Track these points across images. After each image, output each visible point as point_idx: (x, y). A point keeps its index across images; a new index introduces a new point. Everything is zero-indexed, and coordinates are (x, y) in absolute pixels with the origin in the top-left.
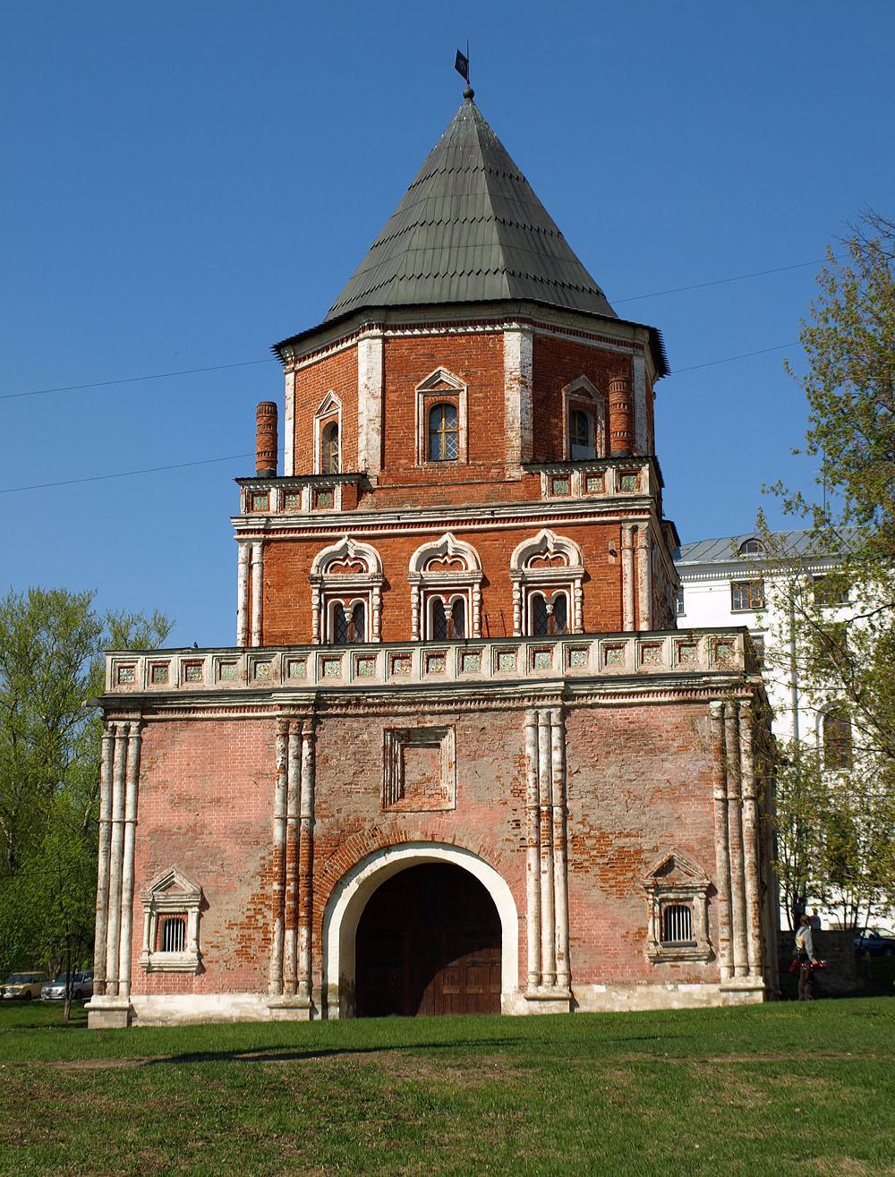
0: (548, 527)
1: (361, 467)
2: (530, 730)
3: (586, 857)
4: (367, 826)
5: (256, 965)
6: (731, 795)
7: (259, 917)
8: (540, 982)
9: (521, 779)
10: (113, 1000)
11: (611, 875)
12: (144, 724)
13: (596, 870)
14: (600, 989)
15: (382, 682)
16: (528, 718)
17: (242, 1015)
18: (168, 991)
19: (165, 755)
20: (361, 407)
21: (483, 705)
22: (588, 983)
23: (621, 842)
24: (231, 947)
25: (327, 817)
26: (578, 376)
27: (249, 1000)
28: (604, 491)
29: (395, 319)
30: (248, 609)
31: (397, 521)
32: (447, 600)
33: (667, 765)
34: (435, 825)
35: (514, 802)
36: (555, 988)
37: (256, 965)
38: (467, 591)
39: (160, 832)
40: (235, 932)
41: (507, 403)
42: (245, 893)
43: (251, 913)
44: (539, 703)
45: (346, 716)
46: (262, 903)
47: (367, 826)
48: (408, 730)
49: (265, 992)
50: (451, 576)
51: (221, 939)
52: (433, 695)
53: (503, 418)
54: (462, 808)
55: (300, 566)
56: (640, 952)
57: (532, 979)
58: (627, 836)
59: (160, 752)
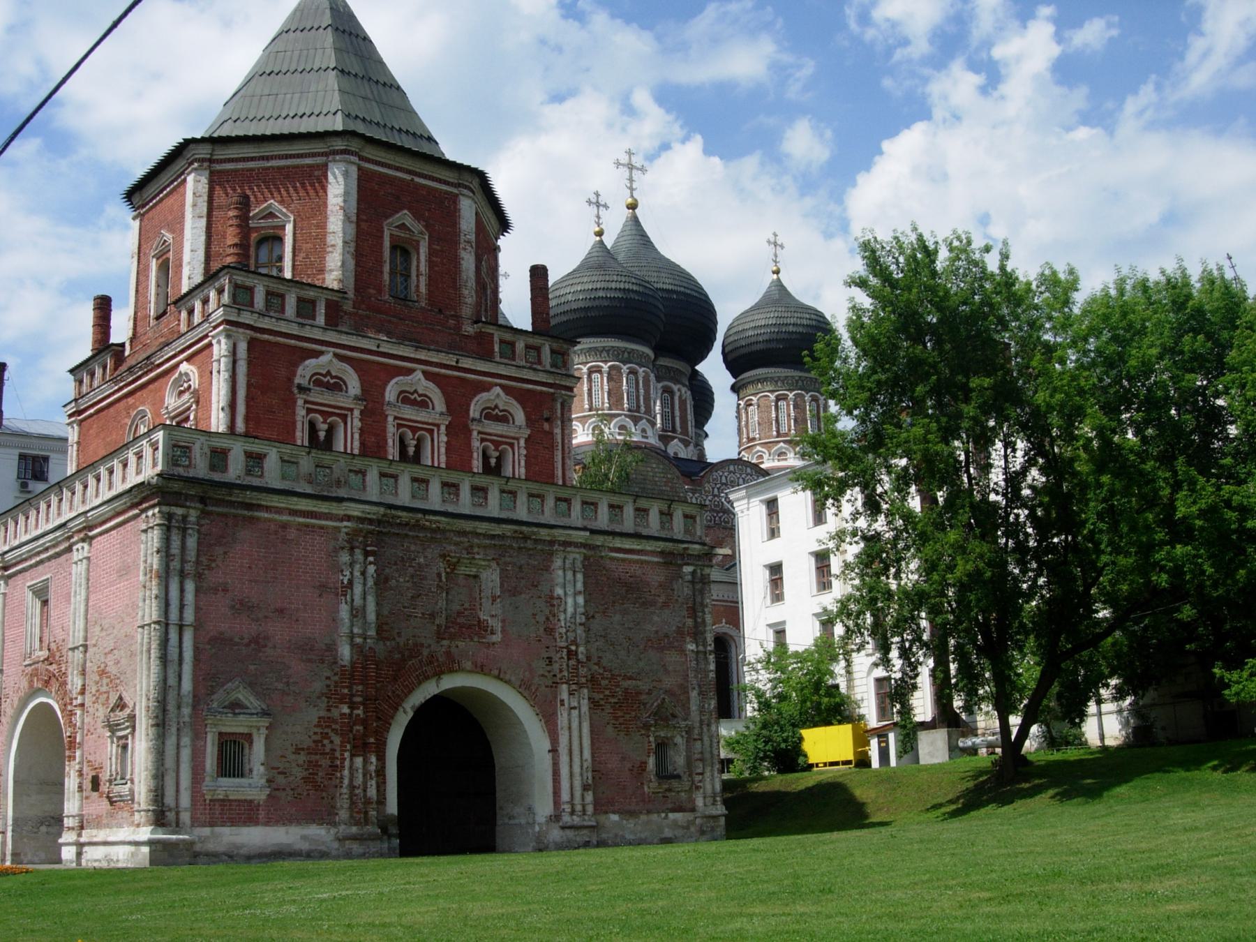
0: (496, 385)
2: (560, 572)
3: (602, 696)
4: (425, 652)
5: (324, 794)
6: (701, 648)
7: (326, 742)
8: (573, 813)
9: (551, 618)
11: (620, 714)
12: (204, 514)
13: (608, 709)
14: (615, 817)
16: (558, 562)
17: (313, 847)
18: (233, 822)
19: (225, 553)
22: (606, 813)
24: (298, 773)
25: (388, 639)
27: (318, 832)
28: (540, 362)
29: (370, 152)
30: (232, 405)
31: (375, 348)
32: (414, 436)
36: (586, 818)
37: (324, 794)
38: (431, 432)
39: (220, 640)
40: (302, 758)
41: (462, 262)
42: (314, 714)
43: (318, 737)
44: (569, 549)
46: (327, 727)
47: (425, 652)
49: (334, 824)
50: (421, 416)
51: (287, 765)
52: (483, 527)
57: (567, 808)
58: (631, 678)
59: (219, 550)
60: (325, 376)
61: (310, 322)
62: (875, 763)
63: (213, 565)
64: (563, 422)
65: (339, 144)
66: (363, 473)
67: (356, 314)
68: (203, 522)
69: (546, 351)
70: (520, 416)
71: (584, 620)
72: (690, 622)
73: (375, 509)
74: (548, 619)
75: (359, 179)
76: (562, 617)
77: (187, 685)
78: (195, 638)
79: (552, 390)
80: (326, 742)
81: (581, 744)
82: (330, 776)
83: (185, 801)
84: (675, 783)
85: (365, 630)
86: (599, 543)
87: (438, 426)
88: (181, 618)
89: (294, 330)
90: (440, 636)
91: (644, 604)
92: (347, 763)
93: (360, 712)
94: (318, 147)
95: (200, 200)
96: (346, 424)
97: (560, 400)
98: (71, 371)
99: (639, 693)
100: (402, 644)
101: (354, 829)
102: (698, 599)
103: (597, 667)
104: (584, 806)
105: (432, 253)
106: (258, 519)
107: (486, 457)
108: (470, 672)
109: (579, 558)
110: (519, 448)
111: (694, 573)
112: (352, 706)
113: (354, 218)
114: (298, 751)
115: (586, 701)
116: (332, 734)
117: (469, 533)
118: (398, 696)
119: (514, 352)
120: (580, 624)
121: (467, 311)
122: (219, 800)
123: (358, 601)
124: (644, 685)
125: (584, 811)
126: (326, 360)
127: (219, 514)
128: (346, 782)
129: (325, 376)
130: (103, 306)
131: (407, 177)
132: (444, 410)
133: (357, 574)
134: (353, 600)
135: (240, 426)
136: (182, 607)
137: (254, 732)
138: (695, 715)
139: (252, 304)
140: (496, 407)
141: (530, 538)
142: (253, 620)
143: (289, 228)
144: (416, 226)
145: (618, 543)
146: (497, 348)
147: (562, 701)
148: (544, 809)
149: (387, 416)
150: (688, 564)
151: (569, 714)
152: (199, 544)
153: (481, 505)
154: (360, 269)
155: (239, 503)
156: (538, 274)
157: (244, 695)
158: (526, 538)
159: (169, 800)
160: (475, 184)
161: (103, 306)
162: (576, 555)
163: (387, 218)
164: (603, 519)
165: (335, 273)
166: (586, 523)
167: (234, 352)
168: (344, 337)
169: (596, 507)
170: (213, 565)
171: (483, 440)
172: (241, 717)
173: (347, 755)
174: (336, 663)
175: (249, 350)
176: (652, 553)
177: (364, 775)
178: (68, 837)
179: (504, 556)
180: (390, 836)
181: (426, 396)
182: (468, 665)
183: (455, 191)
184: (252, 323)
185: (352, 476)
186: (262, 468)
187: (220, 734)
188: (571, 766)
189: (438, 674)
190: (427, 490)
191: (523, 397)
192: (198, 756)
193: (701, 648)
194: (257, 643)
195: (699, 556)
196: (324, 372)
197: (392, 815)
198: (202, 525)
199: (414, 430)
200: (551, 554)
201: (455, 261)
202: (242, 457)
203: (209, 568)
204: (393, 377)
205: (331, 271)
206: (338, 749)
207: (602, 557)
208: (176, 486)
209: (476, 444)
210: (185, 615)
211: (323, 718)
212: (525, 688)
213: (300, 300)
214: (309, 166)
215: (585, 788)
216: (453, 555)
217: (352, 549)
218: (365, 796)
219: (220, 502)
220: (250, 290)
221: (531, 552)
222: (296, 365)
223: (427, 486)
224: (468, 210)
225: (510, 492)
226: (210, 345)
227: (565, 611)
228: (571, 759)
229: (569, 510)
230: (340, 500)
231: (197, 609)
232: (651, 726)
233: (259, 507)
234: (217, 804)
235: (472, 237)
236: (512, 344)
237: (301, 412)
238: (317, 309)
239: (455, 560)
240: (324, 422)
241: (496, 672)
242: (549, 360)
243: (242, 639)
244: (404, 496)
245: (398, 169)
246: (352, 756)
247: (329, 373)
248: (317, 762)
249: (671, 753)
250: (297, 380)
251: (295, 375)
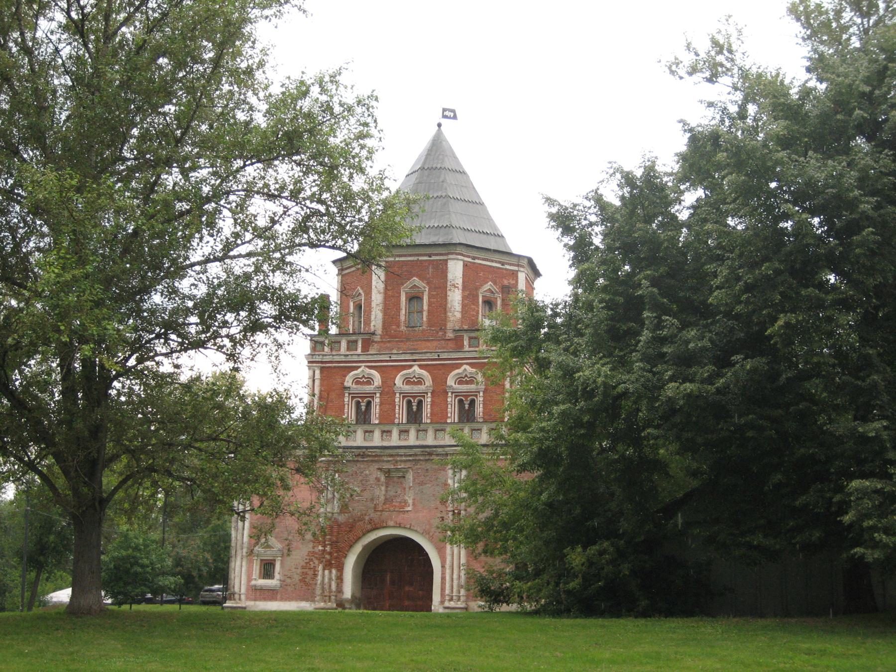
1: (372, 329)
4: (367, 518)
7: (311, 563)
10: (237, 603)
18: (265, 599)
20: (373, 298)
21: (427, 458)
24: (297, 578)
26: (487, 282)
34: (400, 518)
35: (442, 508)
36: (459, 603)
40: (299, 571)
43: (307, 561)
47: (367, 518)
48: (389, 469)
49: (313, 601)
53: (446, 305)
55: (339, 381)
57: (447, 598)
67: (382, 342)
80: (311, 563)
83: (243, 590)
87: (427, 393)
89: (343, 358)
90: (376, 511)
92: (320, 573)
93: (328, 549)
112: (325, 546)
113: (382, 291)
116: (314, 559)
117: (396, 455)
121: (450, 325)
126: (362, 370)
128: (319, 582)
131: (415, 258)
140: (466, 376)
146: (466, 343)
153: (406, 439)
158: (430, 454)
175: (321, 372)
182: (391, 523)
183: (445, 258)
187: (262, 560)
213: (349, 342)
222: (345, 376)
235: (459, 281)
241: (408, 526)
245: (410, 255)
246: (324, 569)
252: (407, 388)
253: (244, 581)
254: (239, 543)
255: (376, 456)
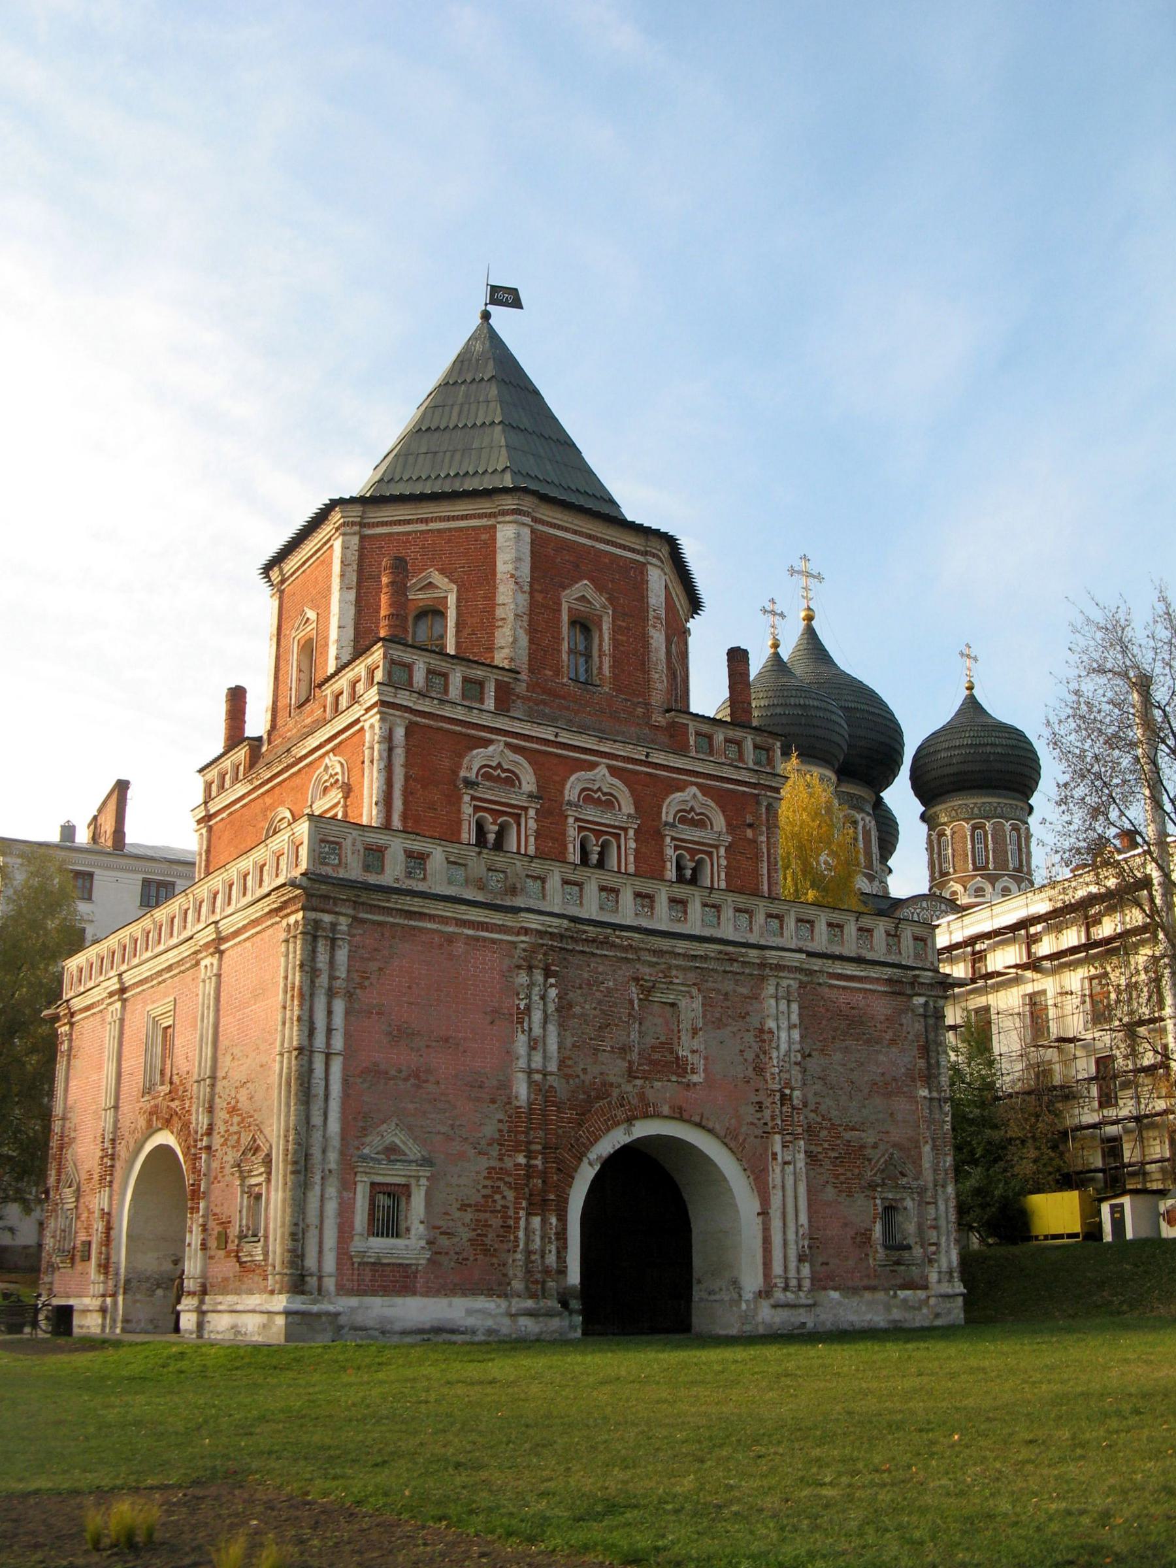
0: (696, 784)
2: (773, 1002)
4: (615, 1093)
5: (495, 1260)
7: (497, 1197)
8: (786, 1288)
9: (762, 1056)
10: (315, 1302)
11: (841, 1170)
13: (827, 1165)
14: (835, 1295)
15: (628, 922)
16: (771, 990)
20: (500, 599)
22: (825, 1289)
23: (848, 1135)
24: (465, 1234)
27: (487, 1305)
28: (741, 758)
29: (547, 513)
31: (552, 738)
32: (597, 841)
33: (882, 1058)
39: (375, 1073)
40: (468, 1216)
41: (651, 641)
43: (488, 1192)
44: (781, 974)
45: (593, 954)
50: (607, 818)
51: (451, 1224)
54: (710, 1082)
55: (447, 763)
56: (867, 1255)
59: (373, 966)
60: (495, 769)
61: (477, 705)
62: (1108, 1237)
63: (367, 983)
64: (768, 829)
65: (509, 503)
66: (543, 880)
68: (355, 931)
69: (749, 745)
70: (719, 822)
71: (799, 1059)
72: (921, 1063)
73: (556, 921)
74: (758, 1056)
75: (532, 543)
76: (775, 1054)
77: (334, 1126)
78: (345, 1069)
79: (756, 792)
80: (497, 1197)
81: (796, 1206)
82: (502, 1238)
84: (906, 1254)
85: (545, 1066)
86: (816, 968)
87: (625, 830)
88: (328, 1044)
89: (459, 714)
91: (868, 1042)
92: (522, 1223)
93: (538, 1162)
94: (485, 506)
95: (350, 569)
96: (519, 825)
97: (765, 804)
98: (201, 771)
99: (862, 1147)
100: (587, 1083)
101: (529, 1303)
102: (932, 1036)
103: (813, 1115)
104: (799, 1280)
105: (616, 630)
106: (421, 929)
107: (680, 868)
108: (666, 1117)
109: (794, 985)
110: (718, 857)
111: (926, 1004)
112: (530, 1156)
113: (527, 588)
114: (463, 1207)
115: (802, 1156)
117: (666, 952)
118: (584, 1144)
119: (711, 746)
120: (796, 1063)
122: (367, 1263)
123: (537, 1031)
124: (870, 1138)
125: (800, 1287)
126: (494, 753)
127: (374, 922)
129: (495, 769)
130: (237, 697)
132: (632, 811)
133: (536, 998)
134: (530, 1029)
135: (397, 823)
136: (329, 1031)
137: (413, 1182)
138: (928, 1176)
139: (411, 683)
140: (692, 809)
141: (736, 960)
142: (412, 1049)
143: (452, 600)
144: (598, 600)
145: (838, 967)
147: (774, 1155)
148: (751, 1281)
149: (566, 817)
150: (920, 995)
151: (783, 1171)
152: (350, 958)
153: (679, 921)
154: (534, 647)
155: (397, 910)
156: (737, 658)
157: (398, 1138)
159: (311, 1262)
160: (664, 551)
161: (237, 697)
162: (790, 982)
163: (564, 588)
164: (821, 940)
165: (506, 651)
166: (801, 944)
167: (388, 739)
168: (517, 724)
169: (812, 926)
170: (367, 983)
171: (676, 848)
172: (398, 1166)
173: (522, 1213)
174: (510, 1103)
176: (877, 980)
177: (542, 1238)
178: (187, 1303)
179: (707, 981)
180: (571, 1312)
181: (611, 795)
184: (410, 705)
185: (530, 882)
186: (425, 870)
187: (373, 1184)
188: (784, 1233)
189: (630, 1120)
190: (617, 902)
191: (724, 799)
192: (345, 1211)
193: (935, 1095)
194: (417, 1077)
195: (931, 985)
196: (494, 764)
197: (574, 1286)
198: (353, 936)
199: (598, 833)
200: (763, 978)
201: (644, 640)
202: (401, 856)
203: (363, 987)
204: (573, 772)
205: (502, 648)
206: (511, 1206)
207: (820, 984)
208: (324, 889)
209: (670, 852)
210: (333, 1042)
211: (494, 1168)
212: (728, 1139)
213: (466, 680)
214: (474, 528)
215: (801, 1259)
216: (647, 977)
217: (530, 968)
218: (543, 1262)
219: (373, 908)
220: (409, 667)
221: (738, 977)
222: (461, 756)
223: (617, 896)
224: (657, 580)
225: (713, 906)
226: (362, 729)
227: (778, 1048)
228: (784, 1224)
229: (782, 928)
230: (516, 910)
231: (347, 1035)
232: (877, 1186)
233: (422, 916)
234: (368, 1269)
236: (710, 737)
237: (467, 810)
238: (486, 690)
239: (650, 984)
240: (494, 823)
242: (752, 757)
243: (400, 1071)
244: (591, 908)
245: (575, 532)
246: (529, 1214)
247: (499, 765)
248: (486, 1221)
249: (899, 1218)
250: (463, 774)
251: (459, 766)
252: (592, 814)
253: (330, 1240)
254: (317, 1136)
255: (625, 949)
